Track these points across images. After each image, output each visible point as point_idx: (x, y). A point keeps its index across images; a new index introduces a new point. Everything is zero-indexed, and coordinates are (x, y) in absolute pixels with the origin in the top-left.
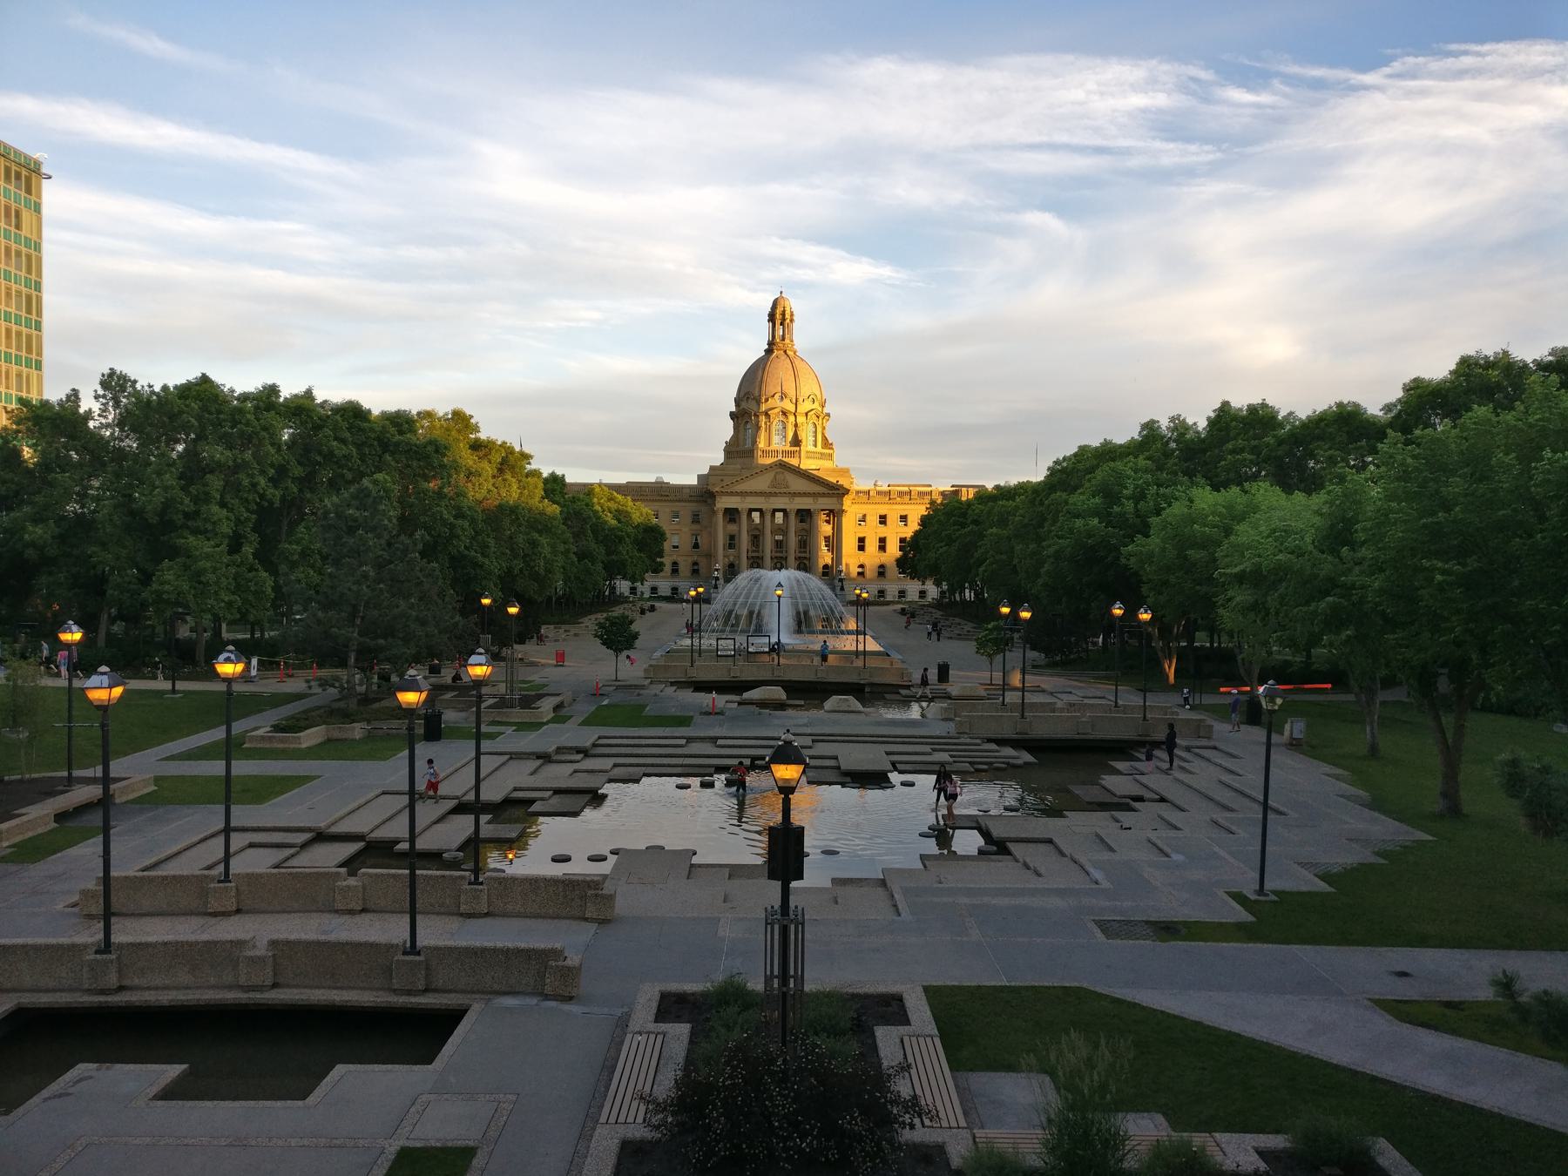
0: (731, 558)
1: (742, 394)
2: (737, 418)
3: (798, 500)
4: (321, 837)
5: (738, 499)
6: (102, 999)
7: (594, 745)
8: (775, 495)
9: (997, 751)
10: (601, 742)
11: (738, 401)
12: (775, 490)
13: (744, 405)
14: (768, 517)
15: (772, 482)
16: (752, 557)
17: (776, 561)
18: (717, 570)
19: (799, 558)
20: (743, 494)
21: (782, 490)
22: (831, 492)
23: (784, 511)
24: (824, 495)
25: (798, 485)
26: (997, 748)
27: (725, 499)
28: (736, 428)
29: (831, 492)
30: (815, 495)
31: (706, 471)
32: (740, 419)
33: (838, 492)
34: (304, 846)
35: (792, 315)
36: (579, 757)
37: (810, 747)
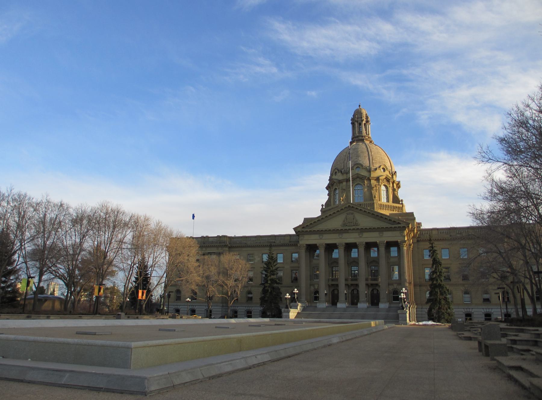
0: (316, 287)
2: (330, 188)
3: (365, 235)
5: (316, 236)
8: (346, 231)
12: (347, 228)
13: (334, 177)
15: (344, 221)
16: (332, 285)
17: (352, 288)
19: (372, 285)
20: (321, 232)
21: (354, 227)
22: (393, 226)
25: (364, 221)
27: (306, 237)
29: (393, 226)
30: (380, 230)
31: (300, 222)
32: (331, 188)
33: (399, 225)
35: (367, 118)
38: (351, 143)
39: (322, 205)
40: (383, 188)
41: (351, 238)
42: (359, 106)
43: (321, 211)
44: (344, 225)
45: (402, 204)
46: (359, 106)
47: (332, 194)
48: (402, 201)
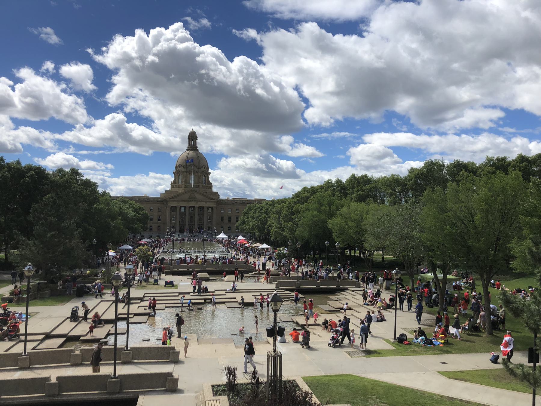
0: (173, 225)
1: (178, 165)
2: (176, 173)
4: (48, 336)
5: (177, 202)
6: (24, 401)
7: (144, 297)
8: (191, 201)
9: (291, 294)
10: (146, 295)
11: (176, 168)
13: (178, 168)
14: (187, 210)
17: (190, 225)
18: (168, 229)
19: (200, 224)
20: (178, 201)
23: (194, 207)
24: (209, 202)
26: (290, 292)
28: (175, 177)
30: (206, 202)
34: (42, 341)
36: (139, 301)
37: (225, 295)
38: (187, 150)
39: (172, 182)
40: (204, 177)
41: (192, 204)
42: (193, 129)
43: (171, 185)
44: (190, 198)
45: (212, 185)
46: (193, 129)
47: (177, 177)
48: (212, 183)
